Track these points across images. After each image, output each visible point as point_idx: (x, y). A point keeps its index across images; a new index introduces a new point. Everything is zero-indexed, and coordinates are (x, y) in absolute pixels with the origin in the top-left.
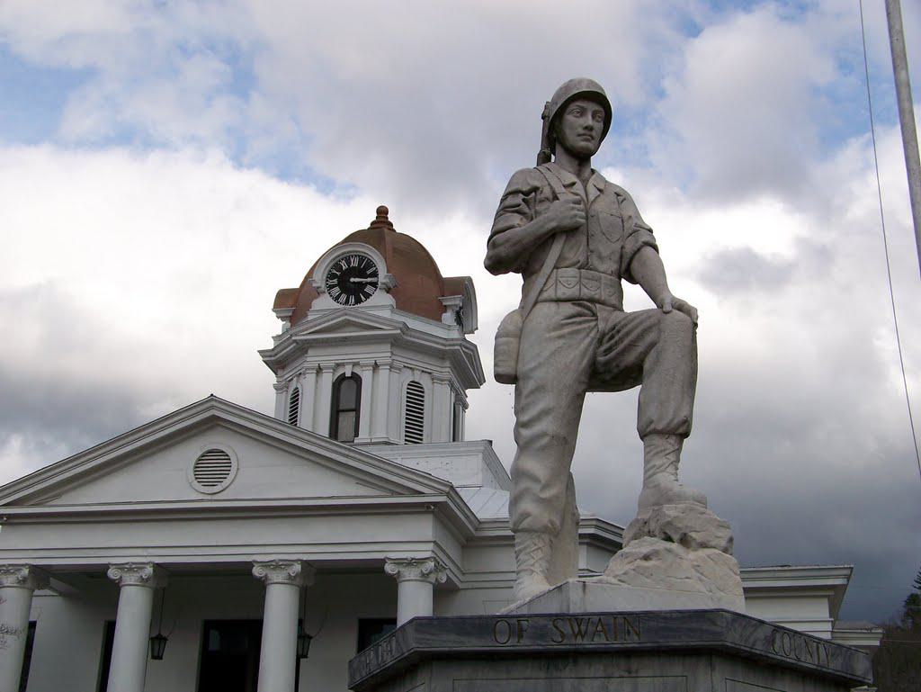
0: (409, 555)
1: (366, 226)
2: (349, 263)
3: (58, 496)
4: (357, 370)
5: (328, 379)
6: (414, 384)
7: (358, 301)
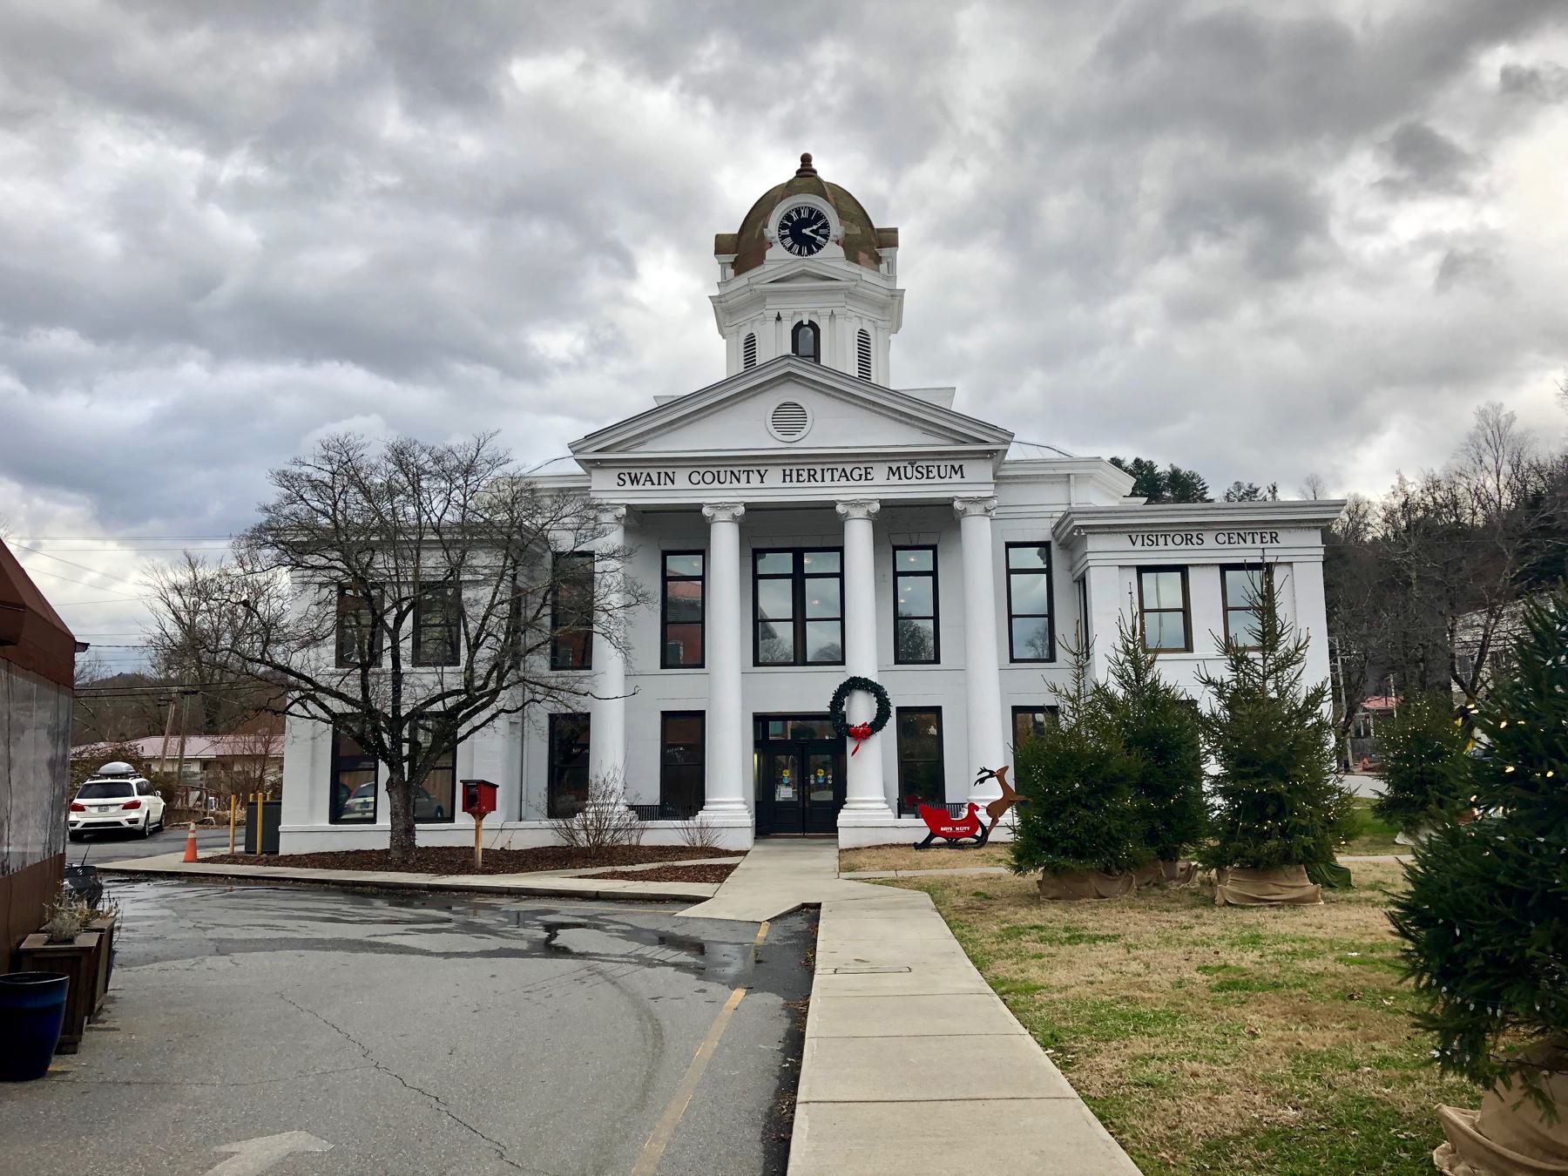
3: (643, 443)
4: (814, 319)
5: (788, 327)
6: (862, 332)
7: (811, 252)
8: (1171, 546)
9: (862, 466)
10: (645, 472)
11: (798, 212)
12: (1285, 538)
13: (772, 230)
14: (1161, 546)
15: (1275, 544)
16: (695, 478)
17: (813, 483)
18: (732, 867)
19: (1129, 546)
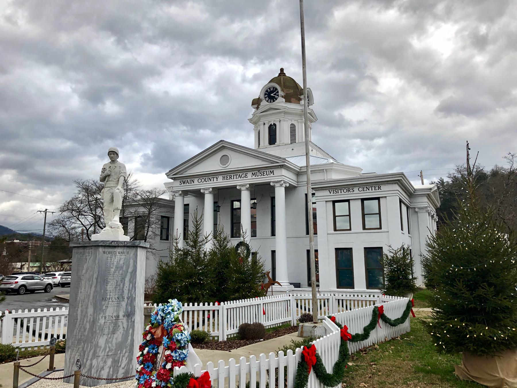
0: (276, 180)
1: (277, 75)
3: (186, 171)
6: (292, 124)
7: (274, 101)
8: (343, 193)
9: (245, 173)
11: (270, 89)
12: (384, 188)
13: (262, 97)
14: (340, 193)
15: (380, 190)
16: (200, 181)
17: (231, 180)
19: (329, 194)
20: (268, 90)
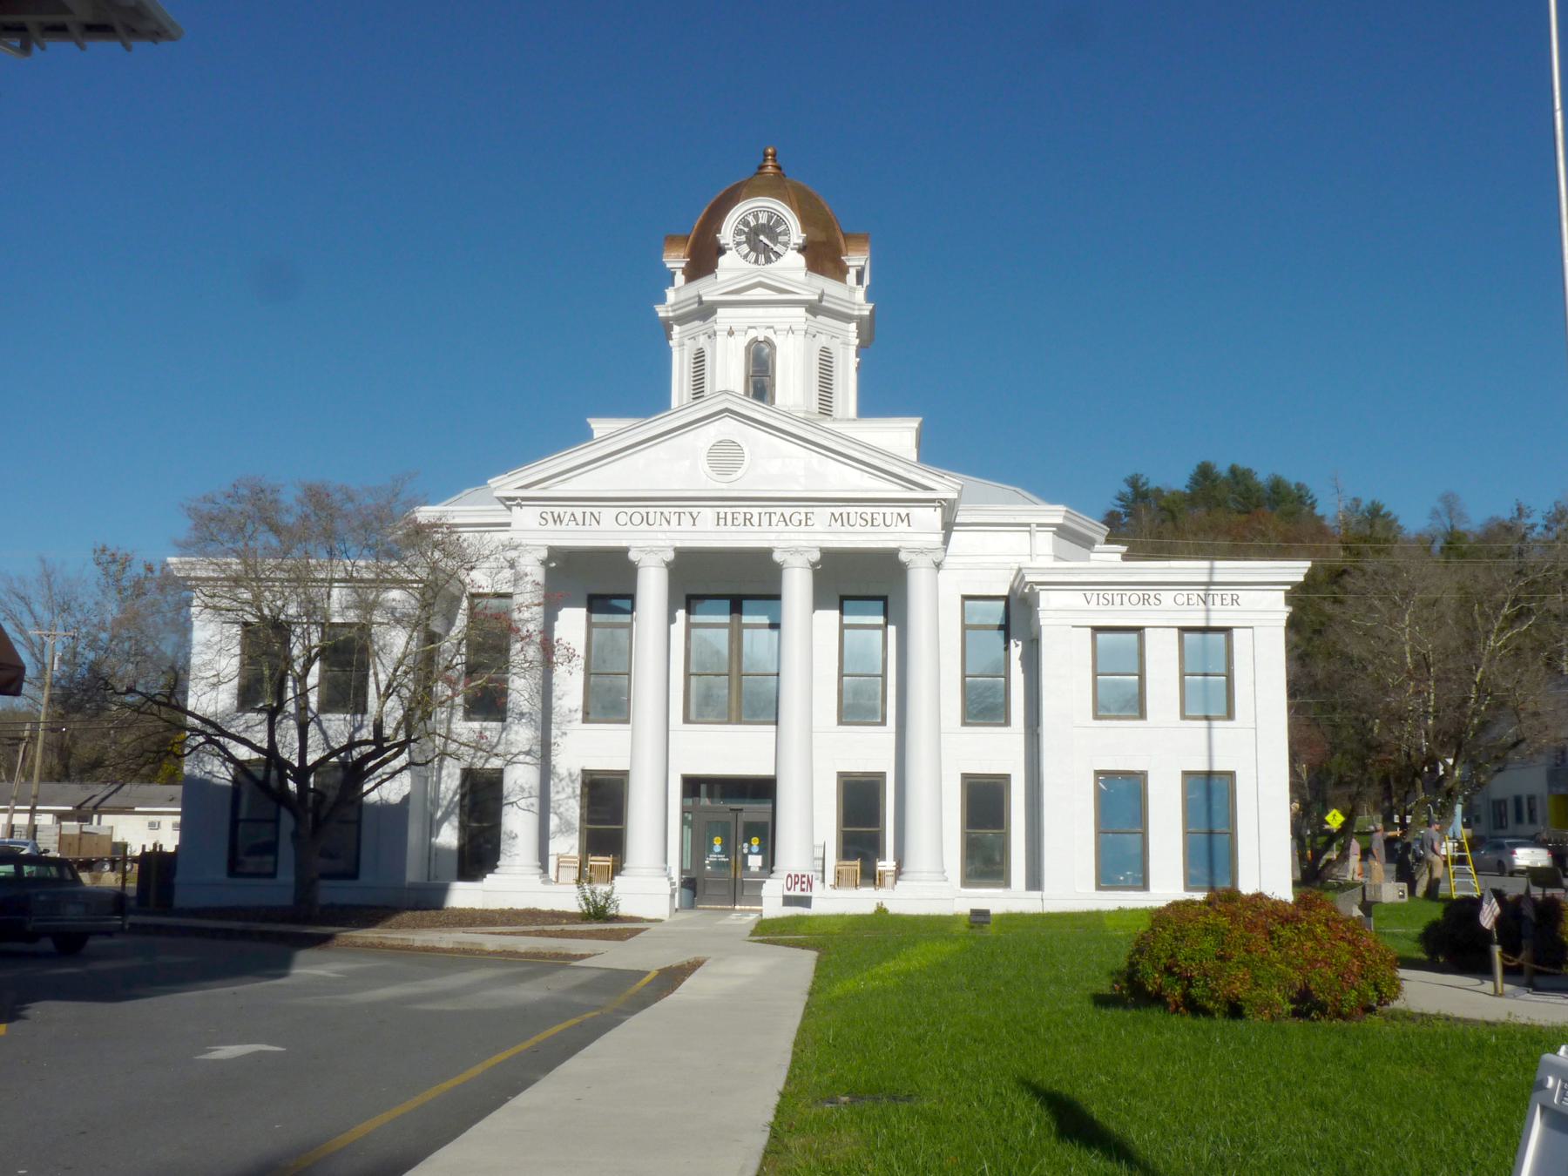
2: (756, 217)
6: (825, 350)
7: (768, 260)
9: (803, 510)
10: (570, 510)
18: (642, 930)
20: (750, 219)
